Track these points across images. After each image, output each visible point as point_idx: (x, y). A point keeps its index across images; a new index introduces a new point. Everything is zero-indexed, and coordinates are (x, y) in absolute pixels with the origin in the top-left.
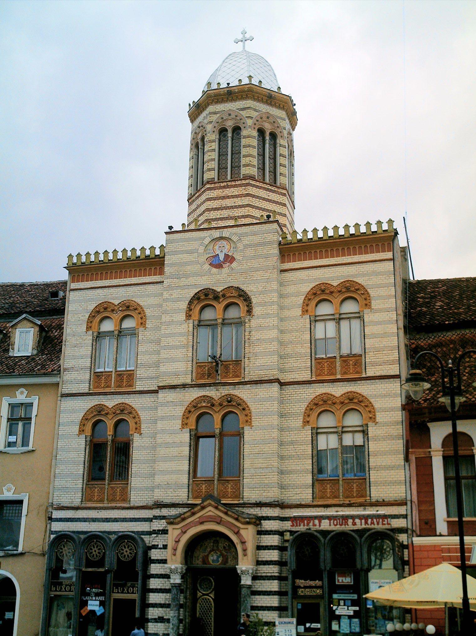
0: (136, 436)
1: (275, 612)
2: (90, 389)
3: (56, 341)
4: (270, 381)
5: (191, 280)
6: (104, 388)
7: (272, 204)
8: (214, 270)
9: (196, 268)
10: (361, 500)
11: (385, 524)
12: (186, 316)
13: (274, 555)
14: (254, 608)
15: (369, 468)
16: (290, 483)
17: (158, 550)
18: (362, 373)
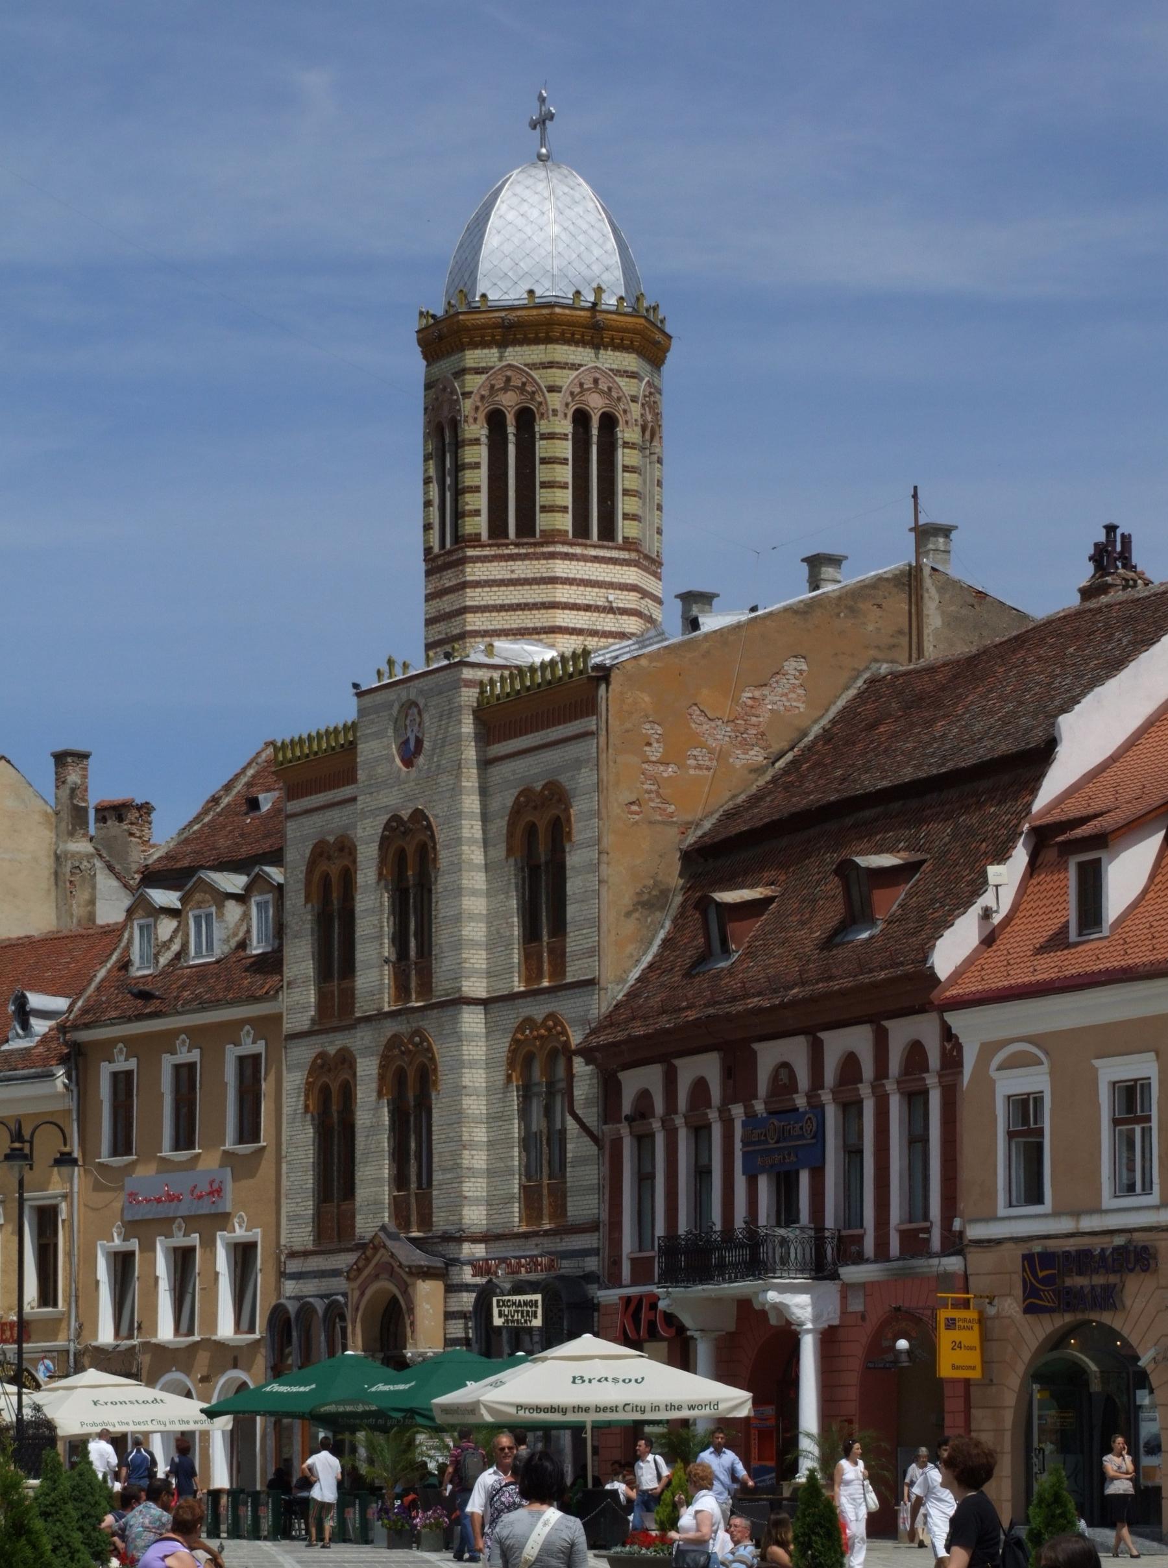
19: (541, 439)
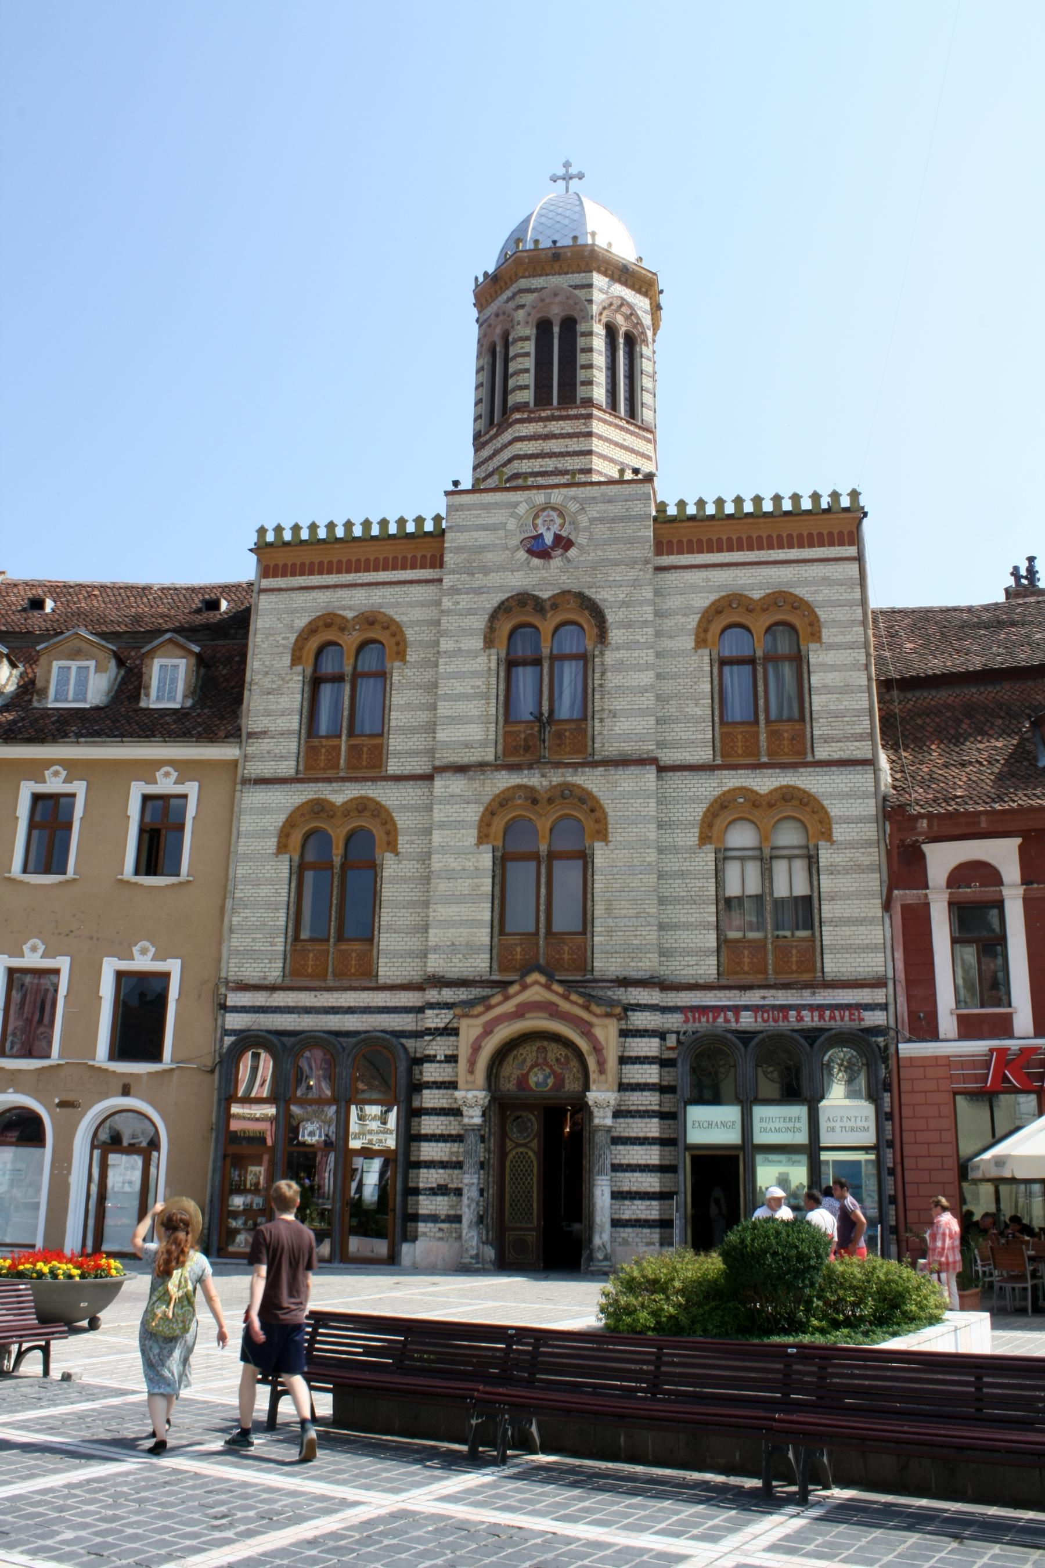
0: (388, 855)
1: (653, 1175)
2: (297, 772)
3: (225, 684)
4: (642, 762)
5: (494, 579)
6: (324, 769)
8: (536, 561)
9: (503, 556)
10: (806, 977)
11: (854, 1020)
12: (485, 642)
13: (651, 1074)
14: (617, 1168)
15: (821, 922)
16: (677, 945)
17: (438, 1065)
18: (805, 754)
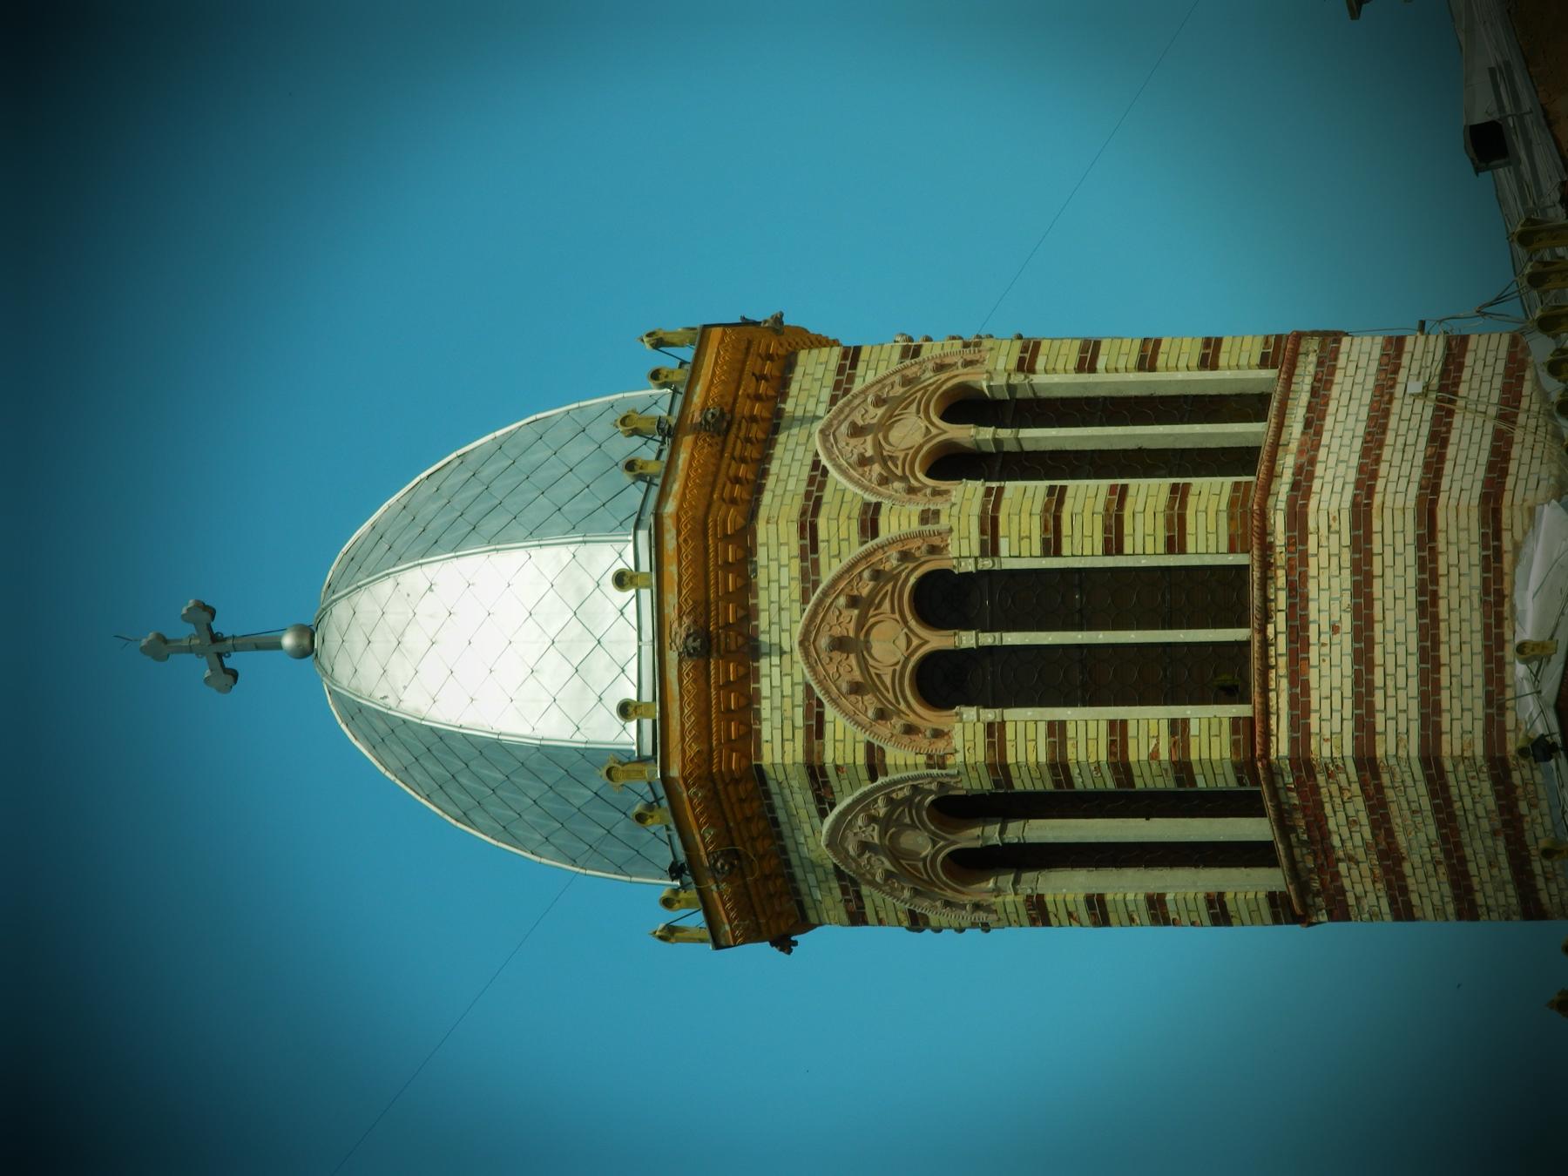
7: (1377, 606)
19: (995, 552)
